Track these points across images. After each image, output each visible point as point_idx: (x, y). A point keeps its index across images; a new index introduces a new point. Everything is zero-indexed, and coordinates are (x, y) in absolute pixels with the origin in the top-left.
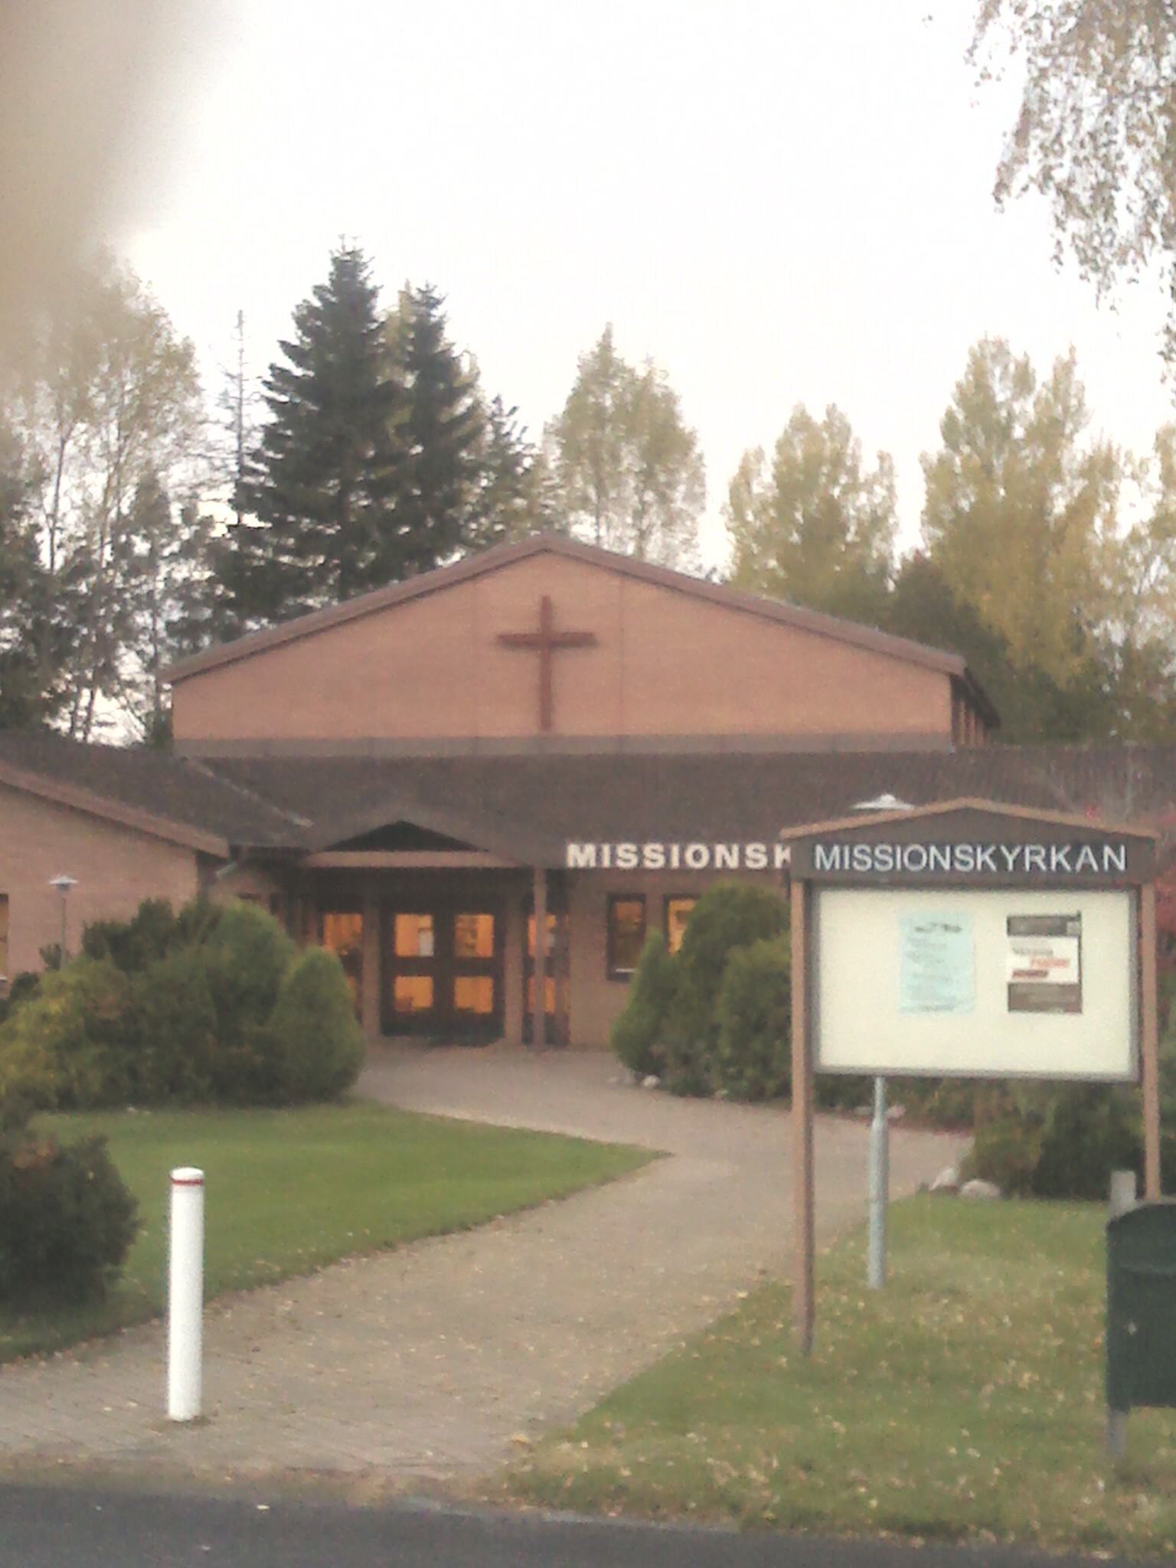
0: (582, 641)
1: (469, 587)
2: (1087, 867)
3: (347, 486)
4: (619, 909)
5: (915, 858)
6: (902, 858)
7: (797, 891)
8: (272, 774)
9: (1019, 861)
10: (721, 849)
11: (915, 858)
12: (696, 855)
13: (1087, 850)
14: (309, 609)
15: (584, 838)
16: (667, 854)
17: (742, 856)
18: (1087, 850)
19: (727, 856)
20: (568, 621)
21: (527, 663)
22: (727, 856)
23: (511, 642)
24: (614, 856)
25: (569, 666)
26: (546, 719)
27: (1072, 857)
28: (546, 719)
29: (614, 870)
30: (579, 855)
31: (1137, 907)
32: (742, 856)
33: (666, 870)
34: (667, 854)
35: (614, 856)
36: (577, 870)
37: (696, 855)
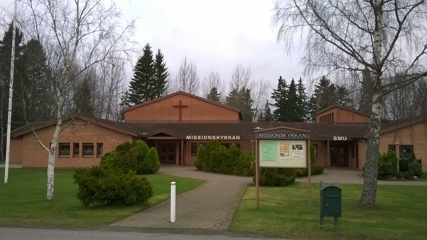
0: (186, 107)
1: (169, 99)
2: (300, 137)
3: (147, 84)
4: (194, 145)
5: (274, 135)
6: (272, 135)
7: (256, 141)
8: (136, 127)
9: (224, 138)
10: (209, 137)
11: (274, 135)
12: (205, 137)
13: (234, 137)
14: (141, 102)
15: (189, 135)
16: (201, 137)
17: (212, 138)
18: (234, 137)
19: (210, 138)
20: (183, 104)
21: (178, 110)
22: (210, 138)
23: (175, 107)
24: (193, 138)
25: (184, 110)
26: (180, 118)
27: (298, 135)
28: (180, 118)
29: (193, 140)
30: (188, 137)
31: (307, 142)
32: (212, 138)
33: (201, 139)
34: (201, 137)
35: (193, 138)
36: (188, 139)
37: (205, 137)
